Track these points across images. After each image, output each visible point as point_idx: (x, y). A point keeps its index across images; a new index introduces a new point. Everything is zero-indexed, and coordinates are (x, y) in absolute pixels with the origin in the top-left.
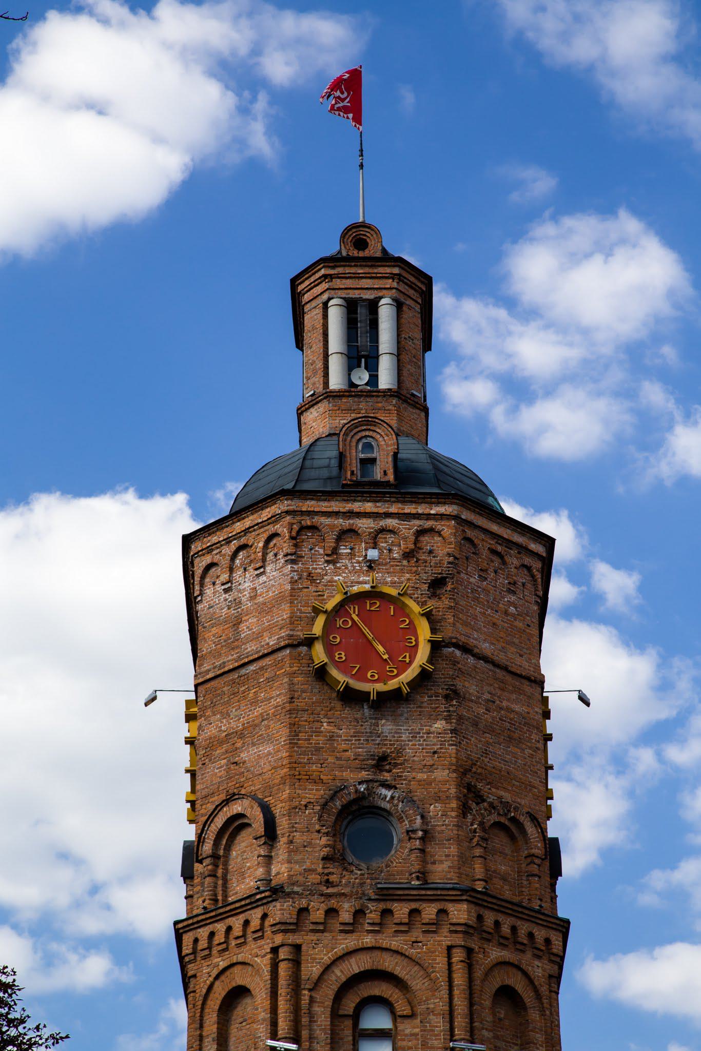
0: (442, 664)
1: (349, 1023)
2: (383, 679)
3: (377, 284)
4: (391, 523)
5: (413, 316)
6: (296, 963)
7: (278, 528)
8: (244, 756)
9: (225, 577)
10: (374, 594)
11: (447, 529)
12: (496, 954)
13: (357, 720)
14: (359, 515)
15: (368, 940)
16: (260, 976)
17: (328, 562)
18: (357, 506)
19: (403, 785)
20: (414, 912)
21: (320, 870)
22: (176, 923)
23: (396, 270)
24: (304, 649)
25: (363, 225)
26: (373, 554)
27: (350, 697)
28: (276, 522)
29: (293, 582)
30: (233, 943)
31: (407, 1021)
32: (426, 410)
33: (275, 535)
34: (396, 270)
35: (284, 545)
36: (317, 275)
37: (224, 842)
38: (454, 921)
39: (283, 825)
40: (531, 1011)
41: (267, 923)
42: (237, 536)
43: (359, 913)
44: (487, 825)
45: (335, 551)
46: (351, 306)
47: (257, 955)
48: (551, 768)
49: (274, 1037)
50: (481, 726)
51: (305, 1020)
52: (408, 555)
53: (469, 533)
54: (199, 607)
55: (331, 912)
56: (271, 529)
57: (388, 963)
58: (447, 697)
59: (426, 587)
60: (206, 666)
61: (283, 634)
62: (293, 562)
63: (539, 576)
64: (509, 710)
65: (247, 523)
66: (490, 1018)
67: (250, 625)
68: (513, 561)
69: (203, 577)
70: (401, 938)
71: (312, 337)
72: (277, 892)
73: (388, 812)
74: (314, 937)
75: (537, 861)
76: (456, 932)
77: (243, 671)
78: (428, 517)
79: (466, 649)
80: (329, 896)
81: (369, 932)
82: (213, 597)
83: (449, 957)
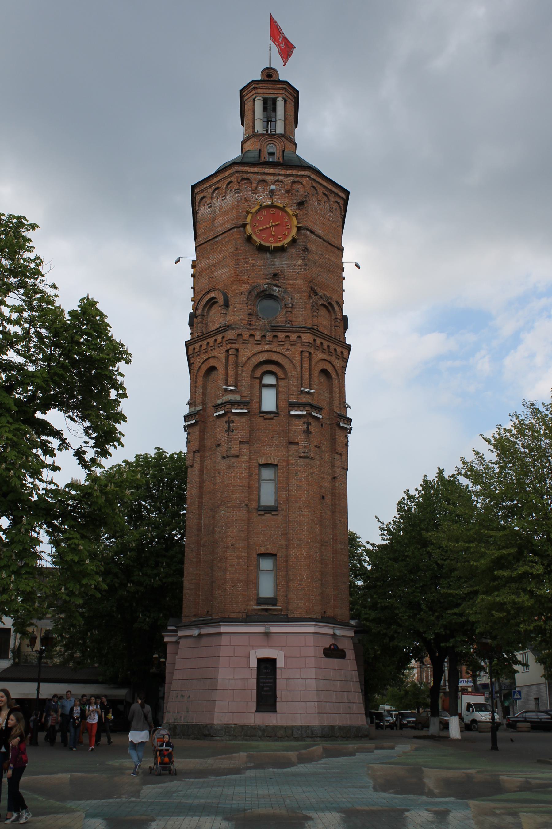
1: (258, 381)
3: (276, 92)
4: (281, 178)
5: (291, 106)
6: (237, 356)
7: (232, 179)
8: (215, 274)
9: (209, 202)
10: (272, 206)
11: (305, 181)
12: (321, 355)
13: (264, 259)
14: (267, 174)
15: (267, 348)
16: (221, 362)
17: (253, 193)
18: (266, 170)
19: (284, 286)
20: (287, 337)
21: (247, 319)
22: (186, 342)
23: (284, 86)
24: (241, 229)
25: (270, 68)
26: (273, 187)
27: (262, 249)
28: (231, 177)
29: (238, 201)
31: (283, 380)
32: (295, 144)
33: (231, 182)
34: (284, 86)
36: (251, 88)
37: (206, 309)
38: (304, 341)
39: (231, 300)
40: (334, 380)
41: (224, 340)
42: (215, 184)
43: (264, 336)
44: (319, 304)
45: (256, 188)
46: (265, 101)
47: (220, 353)
48: (344, 290)
49: (227, 385)
50: (317, 264)
51: (239, 379)
52: (288, 192)
54: (198, 215)
55: (252, 336)
57: (275, 357)
58: (303, 250)
59: (295, 205)
60: (200, 239)
61: (233, 222)
62: (238, 193)
63: (342, 207)
64: (329, 259)
65: (219, 178)
66: (317, 381)
68: (332, 199)
69: (200, 203)
70: (281, 347)
71: (248, 114)
72: (228, 327)
73: (277, 297)
74: (245, 346)
75: (338, 321)
76: (305, 345)
77: (216, 240)
78: (297, 176)
79: (312, 232)
80: (250, 329)
81: (267, 344)
82: (204, 211)
83: (301, 355)
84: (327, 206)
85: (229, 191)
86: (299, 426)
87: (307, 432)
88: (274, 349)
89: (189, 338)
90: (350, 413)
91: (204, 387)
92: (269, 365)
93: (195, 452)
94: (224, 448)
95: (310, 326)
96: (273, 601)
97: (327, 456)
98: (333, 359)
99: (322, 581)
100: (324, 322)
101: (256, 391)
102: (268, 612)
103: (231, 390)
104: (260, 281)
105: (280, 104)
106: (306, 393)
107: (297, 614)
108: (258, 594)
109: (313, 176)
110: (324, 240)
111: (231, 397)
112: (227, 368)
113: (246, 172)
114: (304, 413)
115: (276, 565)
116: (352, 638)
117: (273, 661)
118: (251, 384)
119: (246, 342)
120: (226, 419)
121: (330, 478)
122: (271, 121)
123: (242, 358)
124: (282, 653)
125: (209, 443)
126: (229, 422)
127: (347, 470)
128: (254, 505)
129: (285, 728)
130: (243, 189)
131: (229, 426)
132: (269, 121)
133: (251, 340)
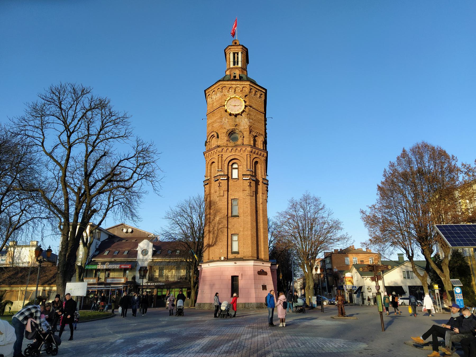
4: (238, 86)
11: (248, 86)
15: (234, 154)
35: (220, 90)
39: (220, 136)
46: (234, 54)
47: (216, 156)
52: (241, 91)
67: (215, 104)
72: (218, 146)
79: (251, 107)
82: (209, 100)
91: (211, 170)
96: (237, 253)
101: (230, 171)
109: (251, 84)
112: (218, 162)
120: (218, 182)
123: (224, 158)
126: (219, 183)
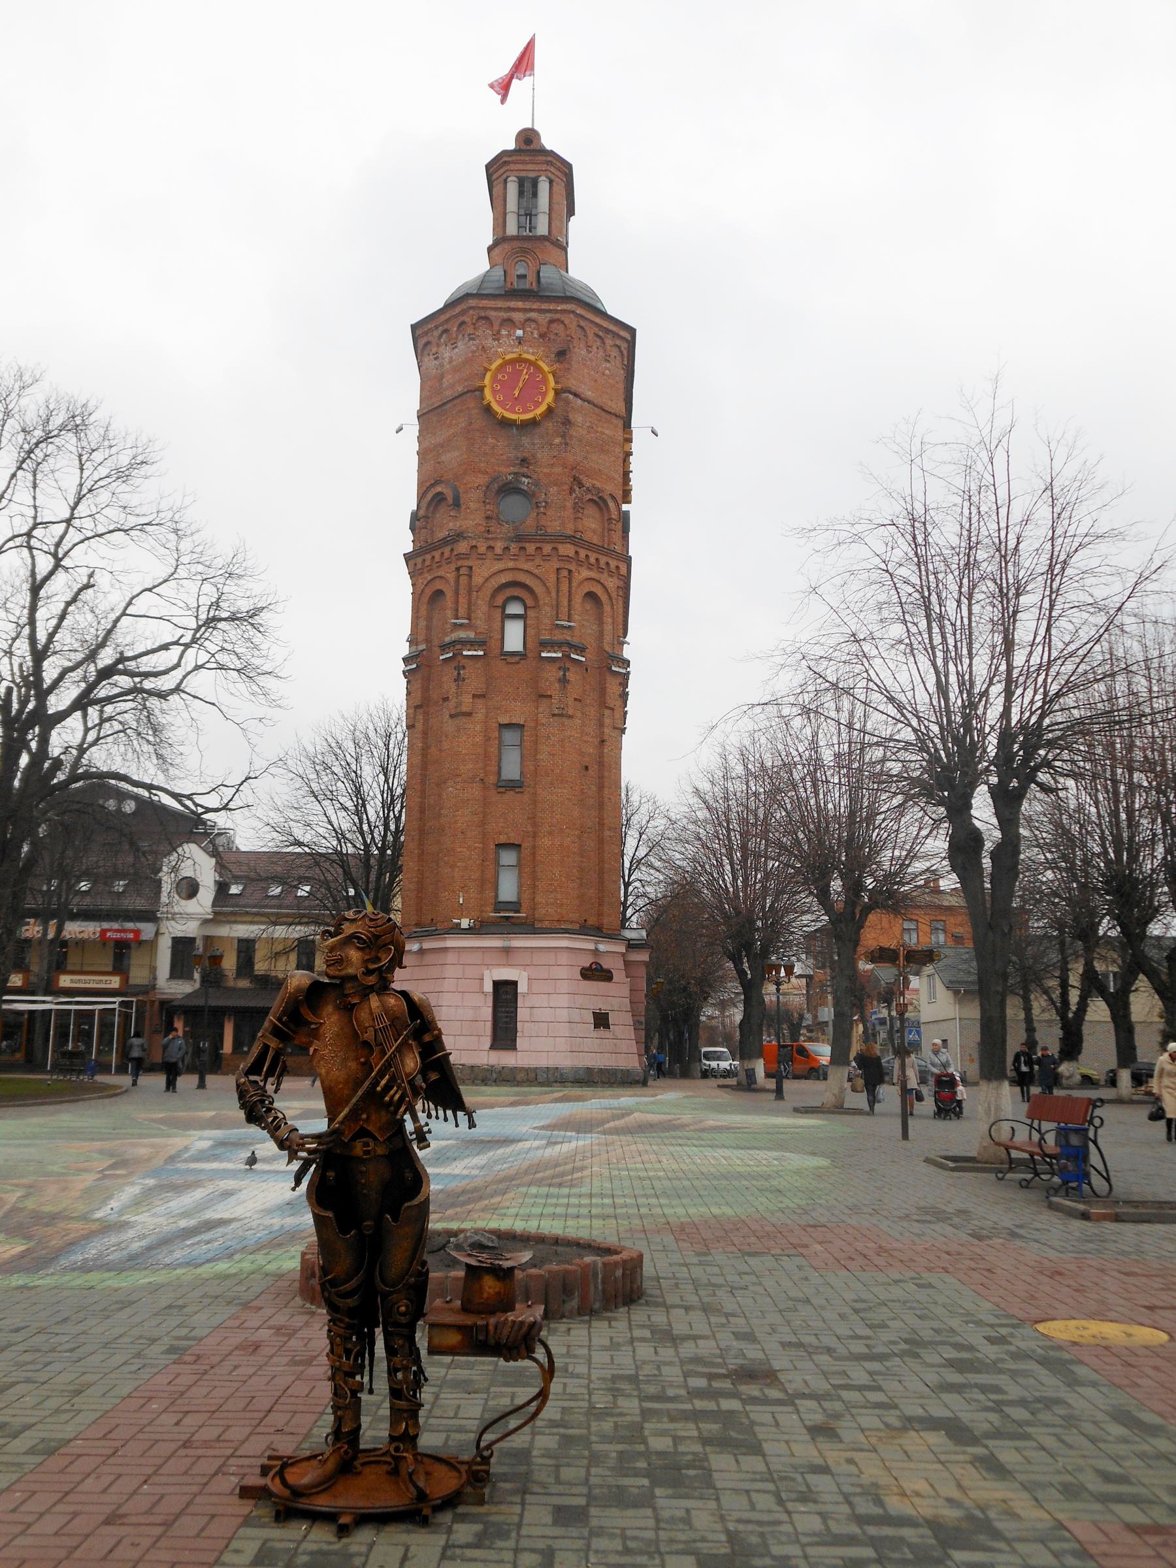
0: (561, 404)
1: (500, 610)
2: (525, 411)
4: (533, 315)
5: (560, 188)
6: (470, 576)
7: (466, 319)
8: (443, 458)
9: (434, 350)
10: (520, 360)
12: (586, 573)
14: (514, 310)
15: (511, 564)
18: (513, 304)
19: (535, 477)
23: (550, 159)
26: (519, 333)
27: (505, 423)
30: (435, 566)
42: (442, 324)
43: (507, 549)
45: (499, 332)
46: (521, 183)
47: (448, 572)
52: (542, 336)
53: (582, 323)
55: (491, 548)
56: (462, 319)
58: (563, 423)
62: (473, 339)
63: (625, 353)
68: (609, 342)
72: (459, 536)
78: (556, 311)
79: (576, 395)
80: (487, 539)
84: (601, 353)
85: (460, 336)
86: (551, 674)
87: (564, 681)
88: (521, 567)
89: (409, 548)
90: (627, 652)
92: (515, 589)
93: (417, 707)
94: (452, 703)
95: (572, 533)
96: (515, 906)
97: (592, 712)
98: (604, 577)
99: (581, 879)
100: (591, 524)
102: (508, 921)
103: (461, 625)
104: (503, 469)
105: (544, 187)
106: (563, 627)
107: (546, 924)
108: (497, 896)
110: (595, 405)
111: (462, 634)
112: (457, 593)
113: (483, 308)
114: (560, 655)
115: (519, 860)
116: (623, 955)
117: (514, 984)
118: (489, 616)
119: (482, 557)
121: (596, 741)
122: (531, 215)
123: (478, 580)
124: (525, 974)
125: (435, 695)
126: (458, 668)
127: (623, 731)
128: (492, 779)
129: (527, 1070)
130: (480, 333)
131: (459, 674)
132: (528, 214)
133: (490, 555)
